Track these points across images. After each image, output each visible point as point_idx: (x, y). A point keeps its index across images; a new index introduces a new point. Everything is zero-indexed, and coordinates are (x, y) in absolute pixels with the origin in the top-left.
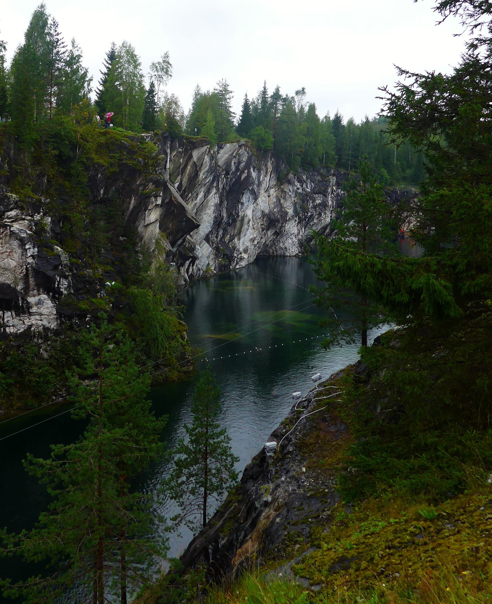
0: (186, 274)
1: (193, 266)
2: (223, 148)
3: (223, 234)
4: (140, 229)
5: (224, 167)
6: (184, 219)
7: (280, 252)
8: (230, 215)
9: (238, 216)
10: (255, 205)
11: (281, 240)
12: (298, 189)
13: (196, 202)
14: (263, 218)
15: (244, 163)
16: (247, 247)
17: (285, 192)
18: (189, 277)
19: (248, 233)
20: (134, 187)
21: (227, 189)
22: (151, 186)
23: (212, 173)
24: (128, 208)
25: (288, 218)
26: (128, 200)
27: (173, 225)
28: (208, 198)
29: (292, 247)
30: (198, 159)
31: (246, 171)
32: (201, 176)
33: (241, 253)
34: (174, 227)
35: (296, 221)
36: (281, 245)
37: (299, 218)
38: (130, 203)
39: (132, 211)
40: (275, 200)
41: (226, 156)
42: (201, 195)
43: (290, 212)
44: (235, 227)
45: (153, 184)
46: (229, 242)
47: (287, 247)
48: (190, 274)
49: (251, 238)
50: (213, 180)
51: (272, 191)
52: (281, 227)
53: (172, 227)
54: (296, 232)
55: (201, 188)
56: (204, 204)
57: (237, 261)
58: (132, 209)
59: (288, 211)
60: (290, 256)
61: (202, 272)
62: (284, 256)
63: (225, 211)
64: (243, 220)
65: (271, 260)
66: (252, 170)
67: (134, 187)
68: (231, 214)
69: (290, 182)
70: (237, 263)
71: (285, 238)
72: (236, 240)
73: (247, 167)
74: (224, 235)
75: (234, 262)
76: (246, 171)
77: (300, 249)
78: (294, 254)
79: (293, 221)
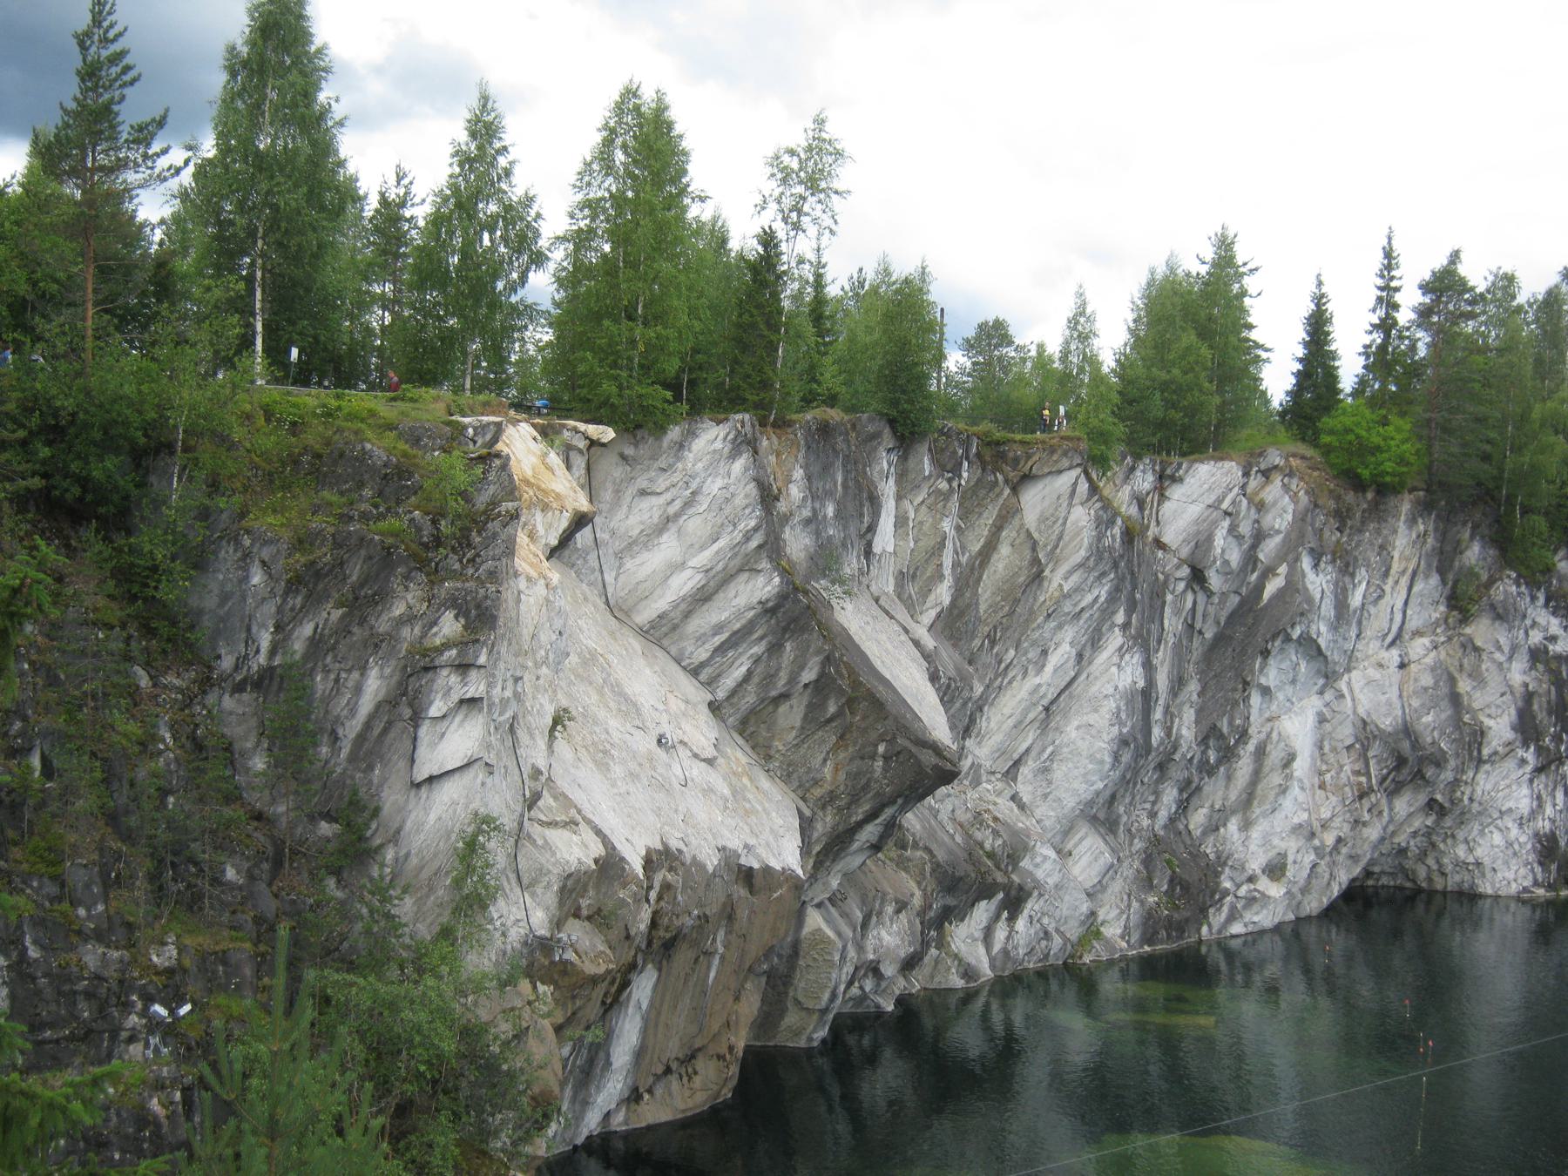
0: (982, 950)
1: (1012, 919)
2: (1181, 480)
3: (1184, 807)
4: (391, 798)
5: (1185, 552)
6: (881, 749)
7: (1457, 878)
8: (1208, 734)
9: (1243, 735)
10: (1329, 696)
11: (1461, 835)
12: (1553, 639)
13: (1037, 680)
14: (1365, 749)
15: (1278, 539)
16: (1283, 855)
17: (1476, 649)
18: (992, 961)
19: (1287, 803)
20: (382, 625)
21: (1209, 635)
22: (449, 626)
23: (1103, 574)
24: (353, 712)
25: (1486, 752)
26: (355, 675)
27: (836, 770)
28: (1092, 668)
29: (1506, 863)
30: (1043, 519)
31: (1283, 569)
32: (1055, 585)
33: (1251, 879)
34: (842, 776)
35: (1523, 761)
36: (1461, 851)
37: (1540, 750)
38: (358, 690)
39: (368, 725)
40: (1427, 680)
41: (1195, 510)
42: (1062, 653)
43: (1500, 729)
44: (1229, 778)
45: (456, 617)
46: (1204, 833)
47: (1486, 861)
48: (997, 947)
49: (1296, 820)
50: (1112, 599)
51: (1418, 647)
52: (1456, 783)
53: (834, 778)
54: (1522, 800)
55: (1060, 627)
56: (1078, 688)
57: (1233, 908)
58: (372, 717)
59: (1488, 722)
60: (1497, 897)
61: (1057, 941)
62: (1470, 897)
63: (1189, 715)
64: (1261, 752)
65: (1420, 908)
66: (1306, 563)
67: (382, 625)
68: (1214, 728)
69: (1501, 615)
70: (1233, 916)
71: (1477, 827)
72: (1233, 826)
73: (1288, 554)
74: (1184, 807)
75: (1219, 909)
76: (1283, 569)
77: (1538, 869)
78: (1514, 889)
79: (1510, 764)
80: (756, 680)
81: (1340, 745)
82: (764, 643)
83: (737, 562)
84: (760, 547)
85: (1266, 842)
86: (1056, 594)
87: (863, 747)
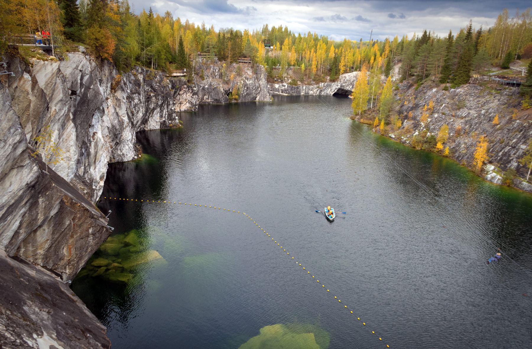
7: (118, 159)
11: (119, 148)
30: (47, 84)
34: (73, 251)
36: (119, 152)
46: (84, 174)
47: (125, 153)
53: (70, 253)
80: (25, 225)
81: (104, 136)
82: (28, 204)
83: (10, 164)
84: (23, 152)
85: (99, 171)
86: (54, 113)
87: (82, 233)
